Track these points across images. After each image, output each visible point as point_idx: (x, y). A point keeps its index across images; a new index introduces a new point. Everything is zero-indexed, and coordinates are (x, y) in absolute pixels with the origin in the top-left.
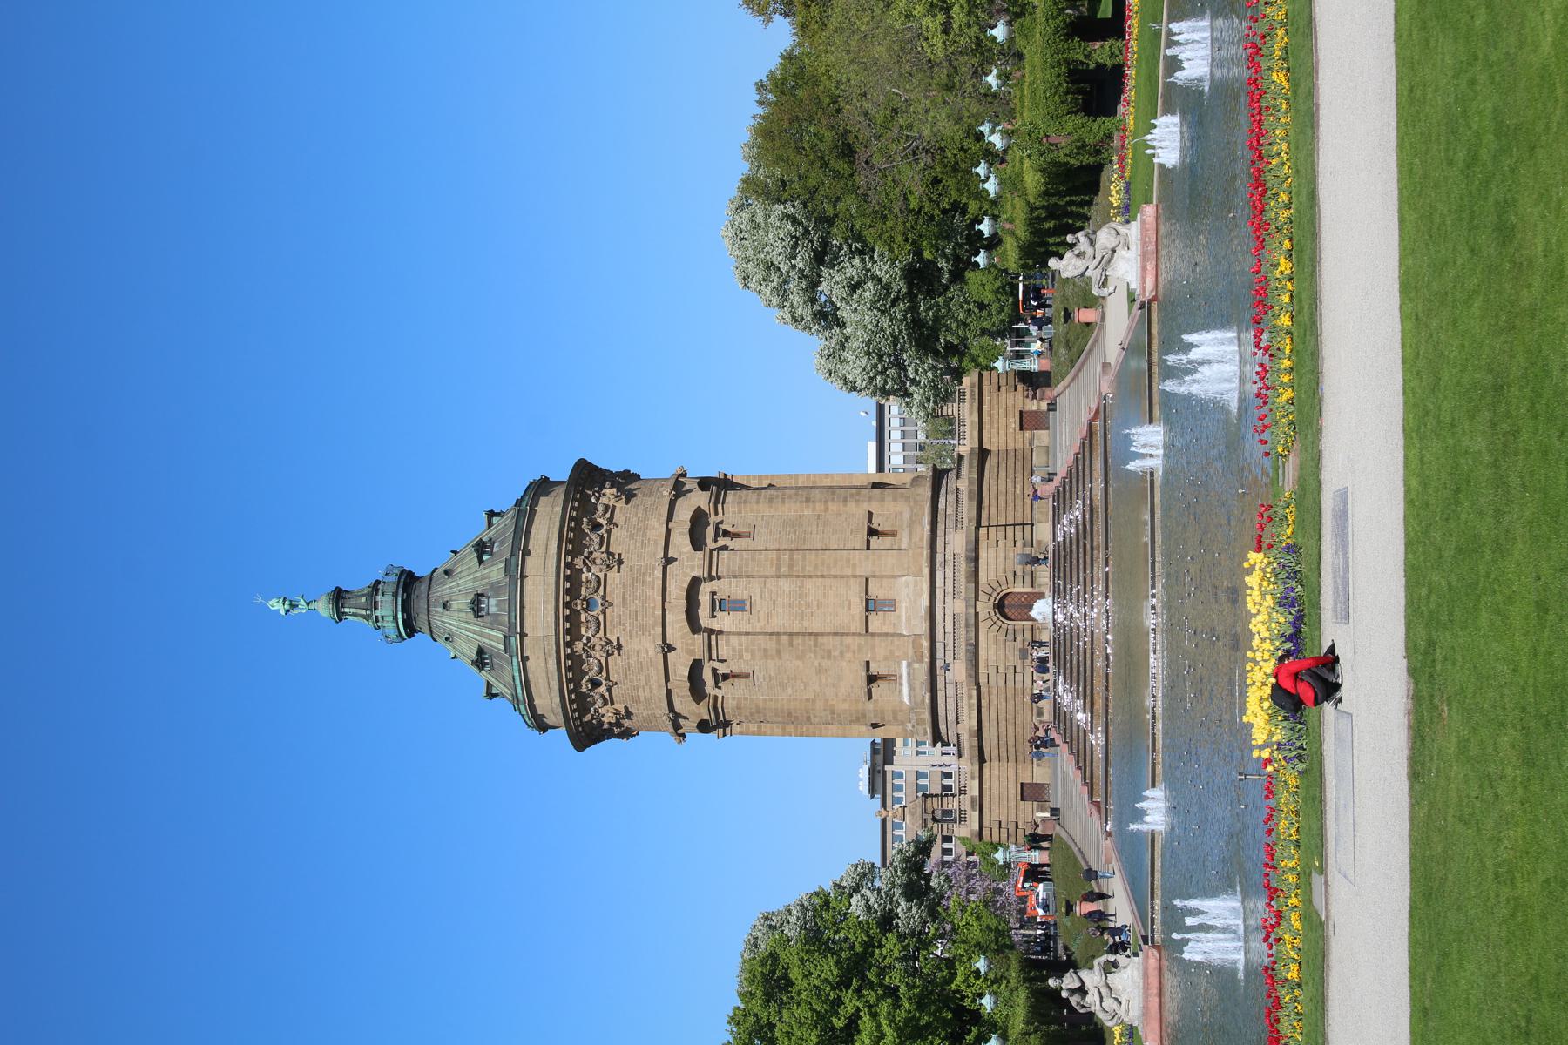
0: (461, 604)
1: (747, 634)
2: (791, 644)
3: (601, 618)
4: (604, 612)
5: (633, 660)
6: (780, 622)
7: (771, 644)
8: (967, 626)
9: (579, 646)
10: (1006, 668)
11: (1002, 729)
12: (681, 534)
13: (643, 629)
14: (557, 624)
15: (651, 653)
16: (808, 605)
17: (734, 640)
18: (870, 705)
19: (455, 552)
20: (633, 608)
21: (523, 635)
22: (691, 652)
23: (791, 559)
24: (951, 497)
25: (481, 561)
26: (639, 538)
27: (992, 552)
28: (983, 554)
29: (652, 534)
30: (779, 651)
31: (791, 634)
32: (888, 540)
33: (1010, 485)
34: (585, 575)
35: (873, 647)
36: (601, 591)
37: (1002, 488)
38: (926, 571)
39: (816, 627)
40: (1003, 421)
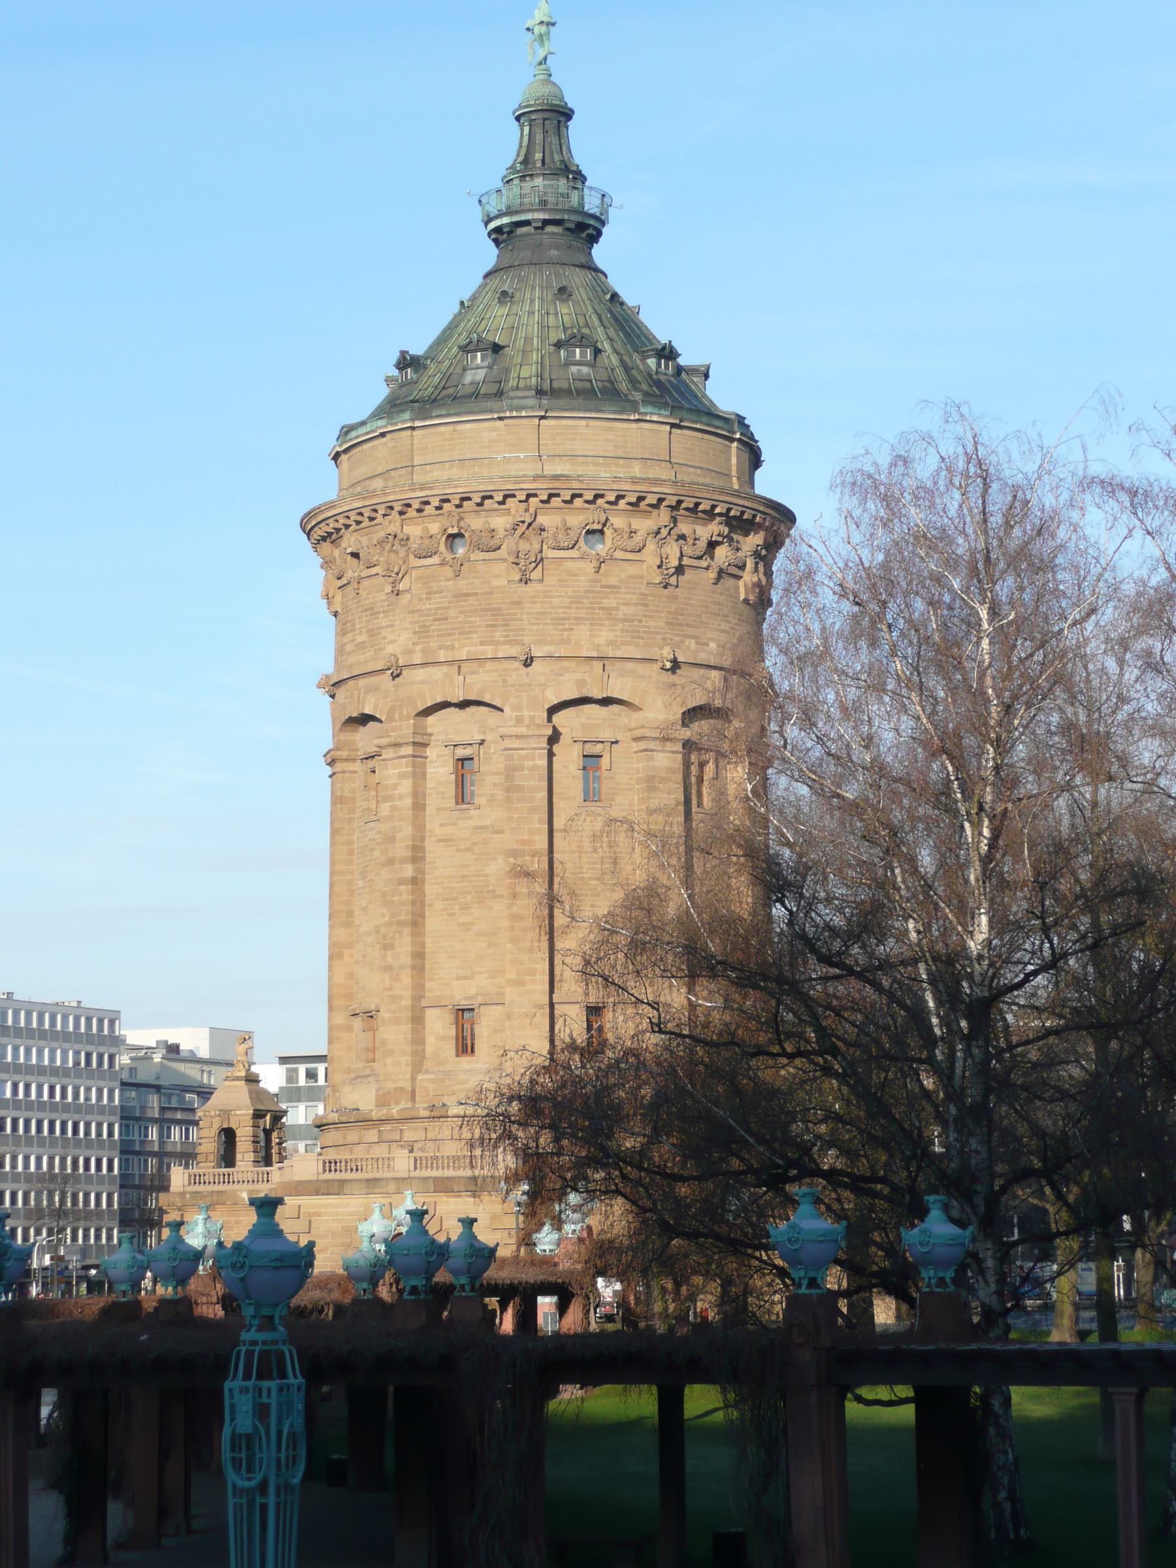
0: (497, 321)
1: (419, 807)
2: (401, 881)
3: (435, 560)
4: (443, 563)
5: (383, 621)
6: (442, 863)
7: (401, 849)
12: (581, 683)
13: (422, 632)
15: (390, 649)
16: (465, 908)
17: (406, 786)
20: (452, 613)
21: (413, 428)
22: (391, 718)
29: (581, 633)
30: (391, 862)
31: (416, 882)
34: (500, 522)
35: (396, 1021)
39: (433, 923)
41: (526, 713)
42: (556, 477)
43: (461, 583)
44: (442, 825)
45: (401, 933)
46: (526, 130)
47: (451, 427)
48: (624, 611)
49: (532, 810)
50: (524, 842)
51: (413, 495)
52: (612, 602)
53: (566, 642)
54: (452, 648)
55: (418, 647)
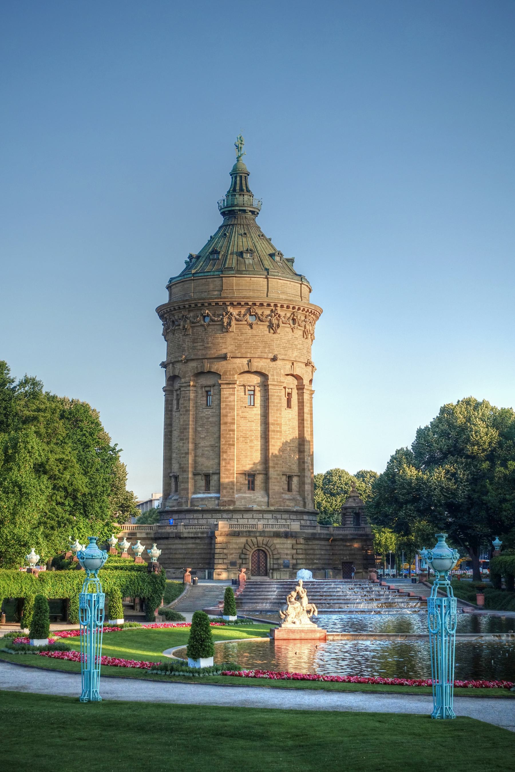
8: (249, 532)
9: (230, 309)
10: (226, 554)
11: (181, 551)
14: (243, 298)
18: (190, 475)
19: (270, 239)
20: (250, 341)
23: (277, 431)
24: (308, 523)
25: (272, 255)
26: (288, 345)
27: (290, 546)
28: (289, 542)
32: (286, 487)
33: (318, 556)
36: (259, 323)
37: (317, 552)
38: (272, 508)
40: (348, 552)
41: (275, 377)
42: (291, 300)
43: (254, 332)
44: (242, 412)
45: (230, 449)
46: (238, 179)
47: (249, 278)
48: (299, 346)
49: (277, 410)
50: (275, 420)
51: (242, 300)
52: (296, 343)
53: (285, 355)
54: (251, 353)
55: (237, 351)
